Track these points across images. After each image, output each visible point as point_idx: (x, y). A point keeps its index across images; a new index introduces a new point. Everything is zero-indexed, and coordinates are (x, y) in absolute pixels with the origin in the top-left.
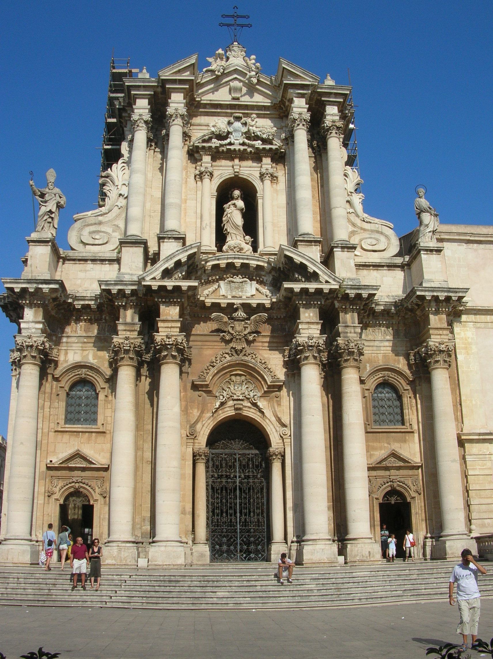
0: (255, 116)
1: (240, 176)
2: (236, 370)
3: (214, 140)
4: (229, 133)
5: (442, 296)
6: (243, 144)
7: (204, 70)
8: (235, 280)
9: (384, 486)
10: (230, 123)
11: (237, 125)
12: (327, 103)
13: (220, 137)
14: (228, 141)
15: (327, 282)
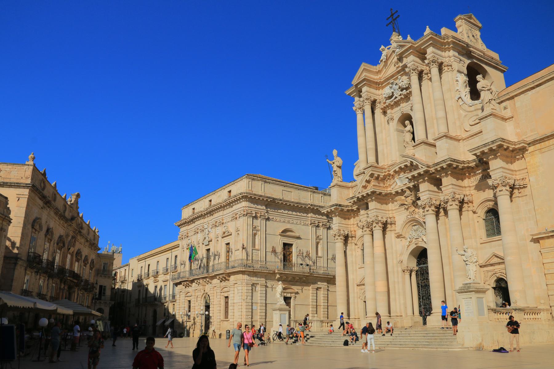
0: (399, 77)
1: (404, 113)
2: (413, 223)
3: (387, 101)
4: (393, 93)
5: (494, 146)
6: (401, 95)
7: (380, 62)
8: (401, 177)
9: (493, 276)
10: (391, 88)
11: (394, 86)
12: (426, 48)
13: (390, 97)
14: (394, 97)
15: (422, 167)
